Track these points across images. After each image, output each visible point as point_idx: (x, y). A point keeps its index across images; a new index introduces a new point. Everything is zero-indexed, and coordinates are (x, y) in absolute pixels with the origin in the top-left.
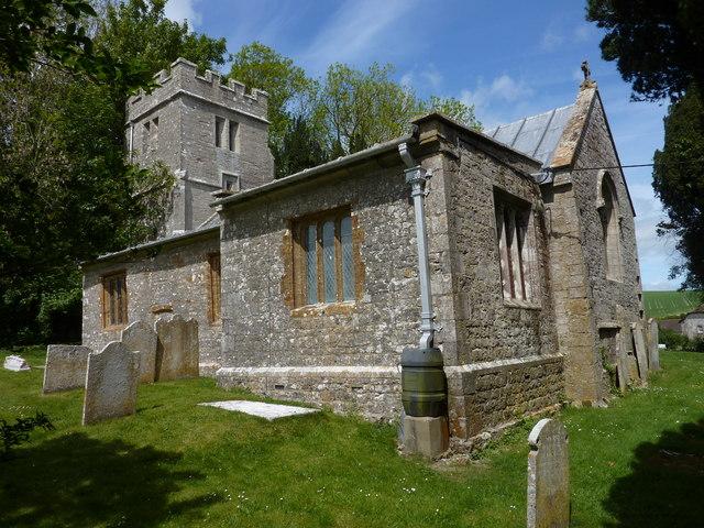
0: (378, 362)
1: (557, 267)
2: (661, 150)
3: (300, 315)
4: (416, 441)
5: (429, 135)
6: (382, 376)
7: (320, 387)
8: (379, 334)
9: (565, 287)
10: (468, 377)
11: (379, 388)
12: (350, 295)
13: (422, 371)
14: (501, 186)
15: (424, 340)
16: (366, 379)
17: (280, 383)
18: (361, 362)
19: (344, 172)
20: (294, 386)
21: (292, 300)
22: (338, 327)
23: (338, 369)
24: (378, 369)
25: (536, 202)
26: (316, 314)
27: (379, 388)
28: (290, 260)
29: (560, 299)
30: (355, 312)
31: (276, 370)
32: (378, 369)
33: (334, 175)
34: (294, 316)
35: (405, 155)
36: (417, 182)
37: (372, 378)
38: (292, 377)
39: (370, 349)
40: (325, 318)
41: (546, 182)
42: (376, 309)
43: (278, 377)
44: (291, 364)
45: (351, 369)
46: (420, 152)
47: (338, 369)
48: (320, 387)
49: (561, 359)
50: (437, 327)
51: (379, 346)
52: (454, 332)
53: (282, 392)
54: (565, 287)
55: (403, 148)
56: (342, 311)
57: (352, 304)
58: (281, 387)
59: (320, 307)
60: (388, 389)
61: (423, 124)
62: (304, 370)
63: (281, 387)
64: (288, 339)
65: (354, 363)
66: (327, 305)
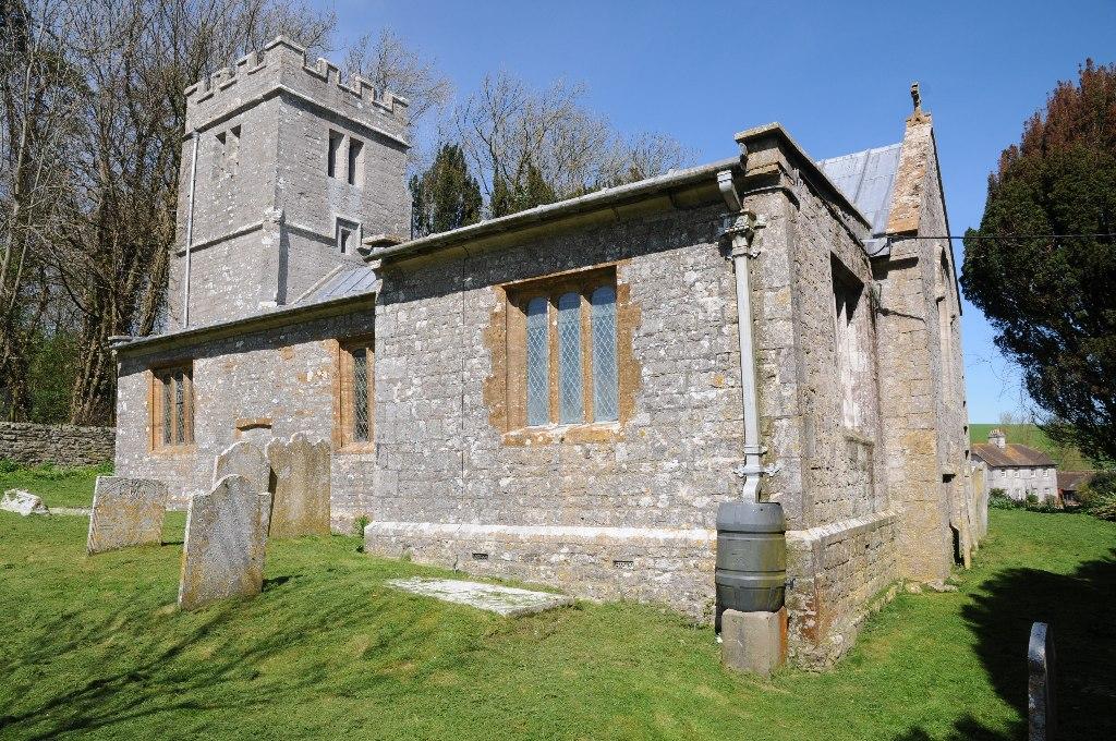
0: (659, 522)
1: (890, 381)
2: (976, 227)
3: (519, 442)
4: (743, 650)
5: (765, 160)
6: (669, 545)
7: (554, 558)
8: (662, 478)
9: (902, 412)
10: (821, 546)
11: (663, 564)
12: (606, 411)
13: (759, 539)
14: (837, 253)
15: (750, 488)
16: (641, 548)
17: (483, 548)
18: (629, 520)
19: (608, 212)
20: (507, 556)
21: (500, 418)
22: (589, 464)
23: (588, 533)
24: (661, 534)
25: (866, 278)
26: (548, 441)
27: (663, 564)
28: (500, 351)
29: (894, 430)
30: (622, 440)
31: (474, 528)
32: (661, 534)
33: (590, 217)
34: (507, 443)
35: (729, 192)
36: (743, 235)
37: (664, 544)
38: (504, 542)
39: (646, 500)
40: (566, 449)
41: (881, 254)
42: (659, 436)
43: (478, 539)
44: (501, 520)
45: (611, 532)
46: (748, 184)
47: (588, 533)
48: (554, 558)
49: (893, 520)
50: (770, 470)
51: (663, 496)
52: (798, 477)
53: (484, 564)
54: (902, 412)
55: (725, 181)
56: (595, 437)
57: (616, 427)
58: (484, 556)
59: (555, 430)
60: (680, 564)
61: (755, 143)
62: (524, 532)
63: (484, 556)
64: (497, 479)
65: (616, 522)
66: (567, 428)
